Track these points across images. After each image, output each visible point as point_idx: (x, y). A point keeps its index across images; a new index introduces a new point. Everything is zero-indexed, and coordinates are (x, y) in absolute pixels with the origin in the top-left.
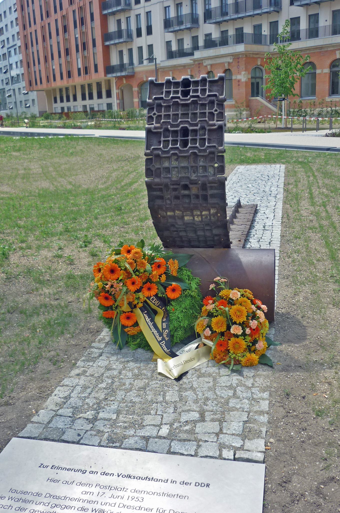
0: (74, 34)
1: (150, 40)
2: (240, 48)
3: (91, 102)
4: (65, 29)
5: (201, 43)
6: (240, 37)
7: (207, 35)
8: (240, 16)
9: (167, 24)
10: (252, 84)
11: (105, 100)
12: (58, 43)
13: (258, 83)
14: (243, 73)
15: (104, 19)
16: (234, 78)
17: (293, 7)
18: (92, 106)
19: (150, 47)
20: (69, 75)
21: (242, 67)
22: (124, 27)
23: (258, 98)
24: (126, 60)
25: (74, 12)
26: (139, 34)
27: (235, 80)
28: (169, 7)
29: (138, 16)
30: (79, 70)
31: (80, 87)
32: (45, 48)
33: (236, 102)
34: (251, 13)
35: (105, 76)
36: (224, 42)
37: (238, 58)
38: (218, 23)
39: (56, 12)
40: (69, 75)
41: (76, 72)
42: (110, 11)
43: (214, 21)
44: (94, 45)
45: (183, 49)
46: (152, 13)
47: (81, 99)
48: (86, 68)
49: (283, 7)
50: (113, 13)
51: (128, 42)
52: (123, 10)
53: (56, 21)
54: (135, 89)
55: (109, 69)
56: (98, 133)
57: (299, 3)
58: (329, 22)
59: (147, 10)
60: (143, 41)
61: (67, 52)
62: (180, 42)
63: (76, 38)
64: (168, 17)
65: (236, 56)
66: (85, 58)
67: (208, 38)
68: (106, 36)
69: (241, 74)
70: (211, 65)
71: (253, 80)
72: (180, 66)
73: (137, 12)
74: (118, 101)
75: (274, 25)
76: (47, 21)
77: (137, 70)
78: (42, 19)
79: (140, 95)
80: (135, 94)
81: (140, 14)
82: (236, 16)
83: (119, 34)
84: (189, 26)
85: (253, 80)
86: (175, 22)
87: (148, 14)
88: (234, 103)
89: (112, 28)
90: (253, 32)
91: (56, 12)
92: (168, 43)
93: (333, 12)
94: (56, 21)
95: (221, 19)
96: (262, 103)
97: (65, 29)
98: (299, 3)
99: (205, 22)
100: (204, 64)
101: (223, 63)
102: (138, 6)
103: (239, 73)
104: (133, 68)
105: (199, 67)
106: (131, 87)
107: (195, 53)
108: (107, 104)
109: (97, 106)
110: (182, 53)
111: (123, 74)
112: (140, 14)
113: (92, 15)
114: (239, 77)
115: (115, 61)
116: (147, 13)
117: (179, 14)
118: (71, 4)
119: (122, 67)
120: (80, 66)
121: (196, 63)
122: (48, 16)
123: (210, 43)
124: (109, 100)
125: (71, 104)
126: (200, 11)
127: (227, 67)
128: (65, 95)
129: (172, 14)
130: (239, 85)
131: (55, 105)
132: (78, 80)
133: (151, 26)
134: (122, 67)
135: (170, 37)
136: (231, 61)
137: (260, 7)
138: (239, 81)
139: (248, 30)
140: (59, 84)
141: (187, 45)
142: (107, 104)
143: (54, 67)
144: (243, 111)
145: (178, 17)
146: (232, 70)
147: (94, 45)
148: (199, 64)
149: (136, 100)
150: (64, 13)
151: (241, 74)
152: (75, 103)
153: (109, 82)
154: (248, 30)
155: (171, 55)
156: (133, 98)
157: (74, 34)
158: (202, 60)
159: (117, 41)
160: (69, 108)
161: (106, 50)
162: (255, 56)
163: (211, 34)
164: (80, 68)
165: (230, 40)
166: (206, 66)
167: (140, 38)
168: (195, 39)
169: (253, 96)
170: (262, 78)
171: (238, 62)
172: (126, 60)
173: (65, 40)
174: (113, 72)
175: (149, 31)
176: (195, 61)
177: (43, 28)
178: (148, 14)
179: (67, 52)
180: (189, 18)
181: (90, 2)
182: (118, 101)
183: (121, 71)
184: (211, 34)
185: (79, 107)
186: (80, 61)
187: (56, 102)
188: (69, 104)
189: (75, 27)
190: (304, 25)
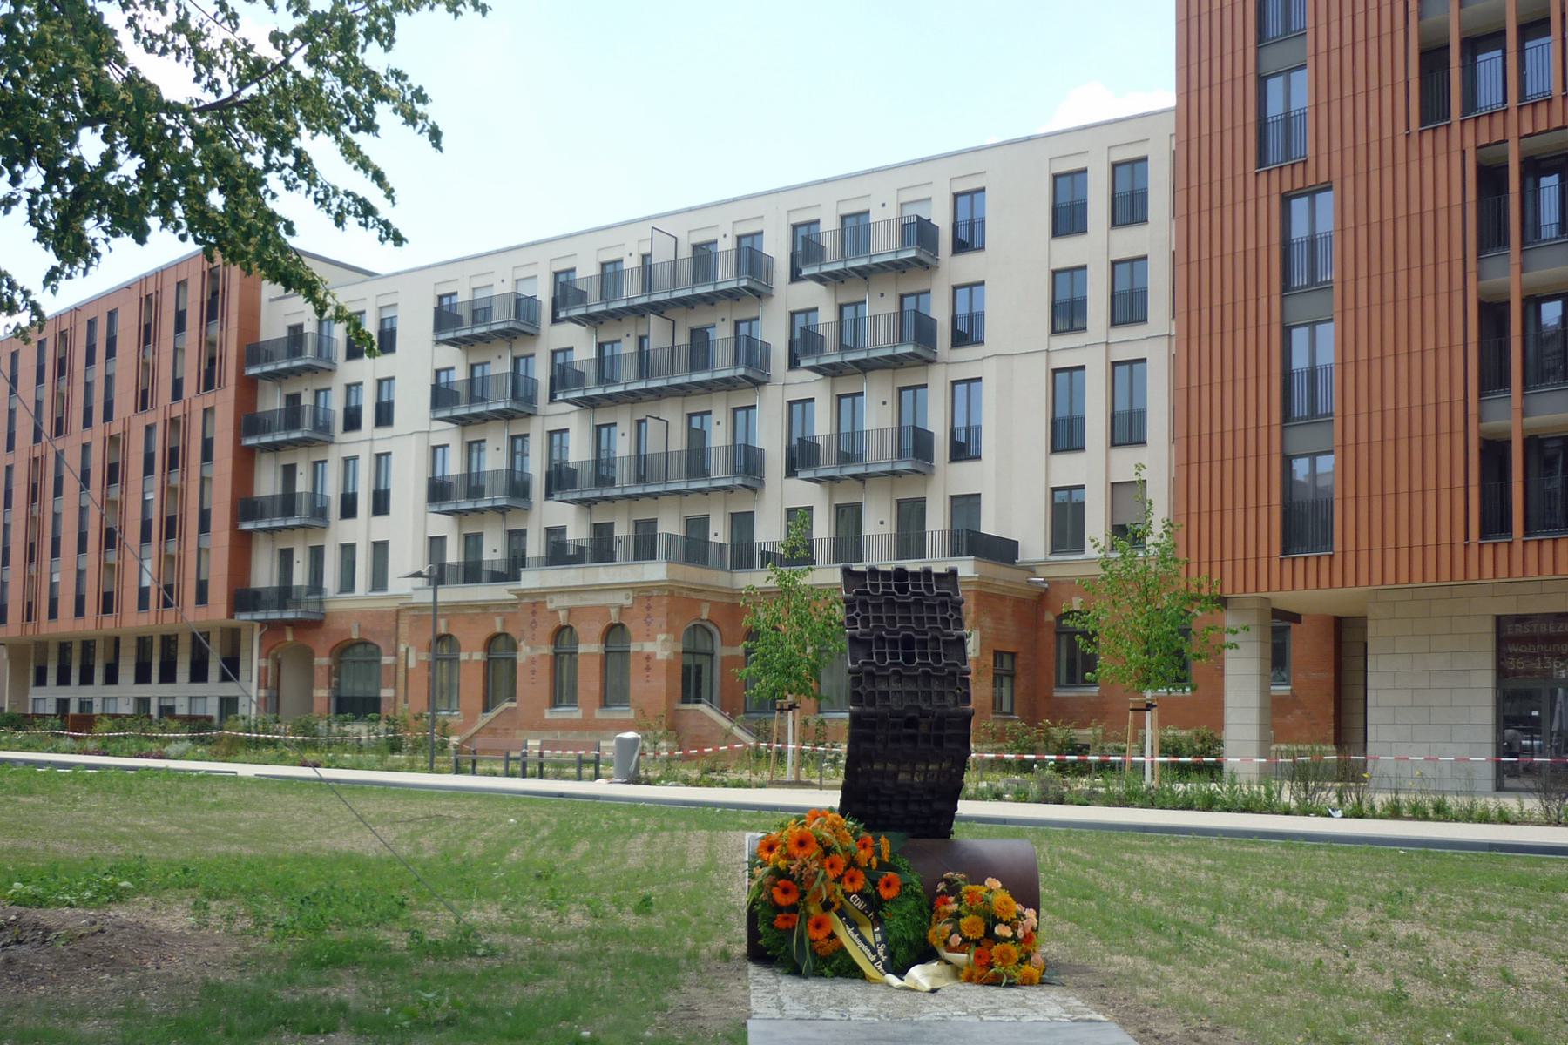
0: (142, 492)
1: (381, 528)
2: (655, 572)
3: (167, 689)
4: (113, 474)
5: (535, 547)
6: (645, 547)
7: (550, 532)
8: (650, 489)
9: (438, 491)
10: (686, 670)
11: (213, 690)
12: (83, 510)
13: (699, 668)
14: (661, 637)
15: (245, 460)
16: (634, 647)
17: (792, 482)
18: (169, 703)
19: (380, 549)
20: (108, 603)
21: (660, 620)
22: (302, 485)
23: (702, 707)
24: (300, 577)
25: (149, 429)
26: (349, 508)
27: (637, 653)
28: (444, 446)
29: (349, 462)
30: (143, 593)
31: (134, 643)
32: (32, 521)
33: (642, 712)
34: (682, 487)
35: (231, 616)
36: (602, 548)
37: (649, 598)
38: (586, 503)
39: (87, 423)
40: (108, 603)
41: (130, 598)
42: (267, 439)
43: (577, 496)
44: (204, 526)
45: (479, 563)
46: (393, 459)
47: (132, 678)
48: (168, 589)
49: (766, 479)
50: (275, 447)
51: (310, 527)
52: (306, 443)
53: (86, 447)
54: (322, 661)
55: (244, 598)
56: (247, 770)
57: (811, 474)
58: (890, 528)
59: (381, 448)
60: (361, 530)
61: (110, 539)
62: (472, 542)
63: (145, 503)
64: (439, 474)
65: (643, 593)
66: (169, 562)
67: (553, 538)
68: (246, 507)
69: (654, 640)
70: (570, 610)
71: (689, 660)
72: (472, 605)
73: (349, 451)
74: (263, 693)
75: (743, 523)
76: (49, 448)
77: (332, 607)
78: (37, 437)
79: (334, 679)
80: (321, 676)
81: (355, 458)
82: (639, 490)
83: (288, 503)
84: (502, 502)
85: (689, 660)
86: (459, 489)
87: (381, 459)
88: (631, 715)
89: (267, 483)
90: (682, 533)
91: (87, 423)
92: (436, 543)
93: (899, 502)
94: (86, 447)
95: (597, 494)
96: (711, 720)
97: (113, 474)
98: (811, 474)
99: (549, 495)
100: (550, 606)
101: (606, 608)
102: (353, 436)
103: (650, 637)
104: (321, 602)
105: (534, 613)
106: (308, 655)
107: (523, 575)
108: (222, 699)
109: (185, 702)
110: (472, 572)
111: (289, 615)
112: (355, 458)
113: (207, 446)
114: (649, 647)
115: (264, 574)
116: (379, 456)
117: (474, 470)
118: (144, 407)
119: (285, 595)
120: (147, 582)
121: (526, 600)
122: (59, 428)
123: (558, 553)
124: (229, 689)
125: (97, 691)
126: (536, 467)
127: (614, 617)
128: (80, 660)
129: (454, 466)
130: (648, 669)
131: (34, 692)
132: (132, 621)
133: (387, 493)
134: (285, 595)
135: (442, 525)
136: (628, 602)
137: (704, 474)
138: (648, 658)
139: (670, 525)
140: (67, 625)
141: (493, 550)
142: (222, 699)
143: (56, 578)
144: (661, 738)
145: (469, 475)
146: (631, 627)
147: (204, 526)
148: (534, 604)
149: (321, 693)
150: (116, 428)
151: (654, 640)
152: (111, 690)
153: (233, 638)
154: (670, 525)
155: (438, 575)
156: (310, 686)
157: (142, 492)
158: (544, 595)
159: (278, 523)
160: (85, 704)
161: (242, 545)
162: (695, 596)
163: (563, 530)
164: (147, 588)
165: (621, 550)
166: (555, 612)
167: (348, 522)
168: (516, 538)
169: (685, 700)
170: (712, 655)
171: (649, 608)
172: (300, 577)
173: (109, 505)
174: (256, 609)
175: (381, 504)
176: (521, 594)
177: (36, 463)
178: (381, 459)
179: (110, 539)
180: (502, 482)
181: (205, 411)
182: (263, 693)
183: (283, 606)
184: (563, 530)
185: (121, 702)
186: (149, 565)
187: (41, 680)
188: (86, 691)
189: (148, 469)
190: (822, 528)
